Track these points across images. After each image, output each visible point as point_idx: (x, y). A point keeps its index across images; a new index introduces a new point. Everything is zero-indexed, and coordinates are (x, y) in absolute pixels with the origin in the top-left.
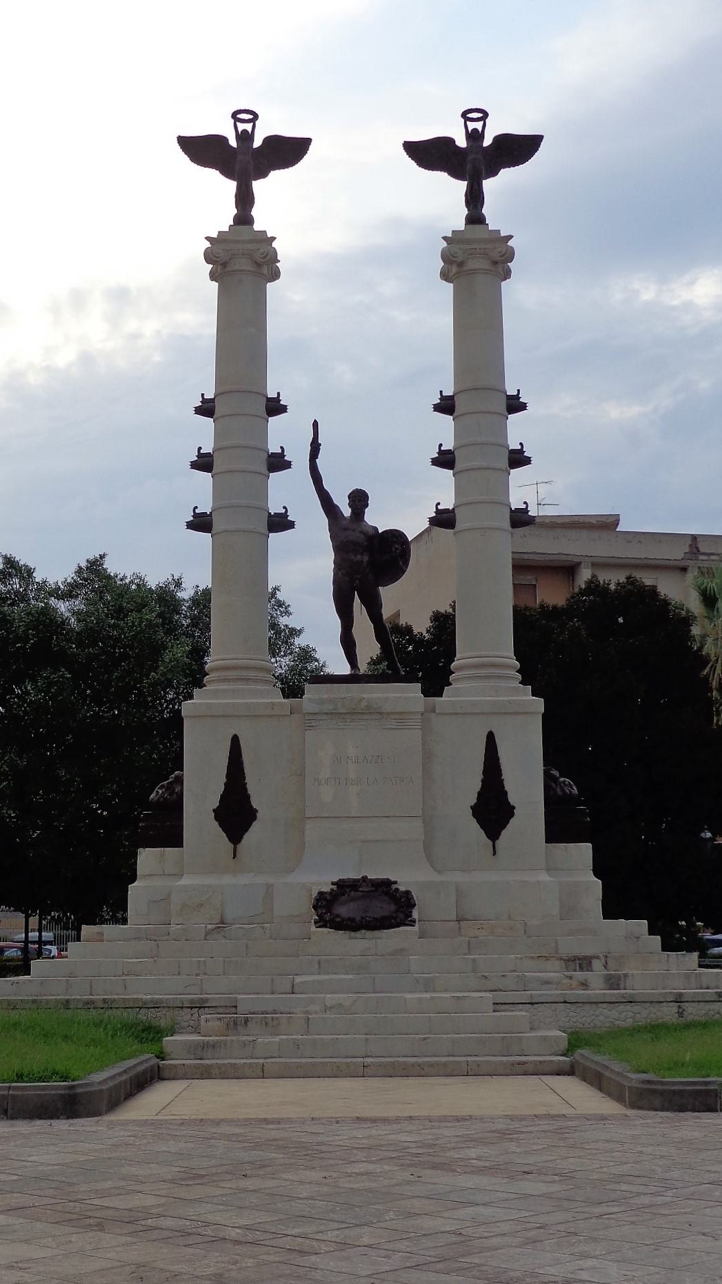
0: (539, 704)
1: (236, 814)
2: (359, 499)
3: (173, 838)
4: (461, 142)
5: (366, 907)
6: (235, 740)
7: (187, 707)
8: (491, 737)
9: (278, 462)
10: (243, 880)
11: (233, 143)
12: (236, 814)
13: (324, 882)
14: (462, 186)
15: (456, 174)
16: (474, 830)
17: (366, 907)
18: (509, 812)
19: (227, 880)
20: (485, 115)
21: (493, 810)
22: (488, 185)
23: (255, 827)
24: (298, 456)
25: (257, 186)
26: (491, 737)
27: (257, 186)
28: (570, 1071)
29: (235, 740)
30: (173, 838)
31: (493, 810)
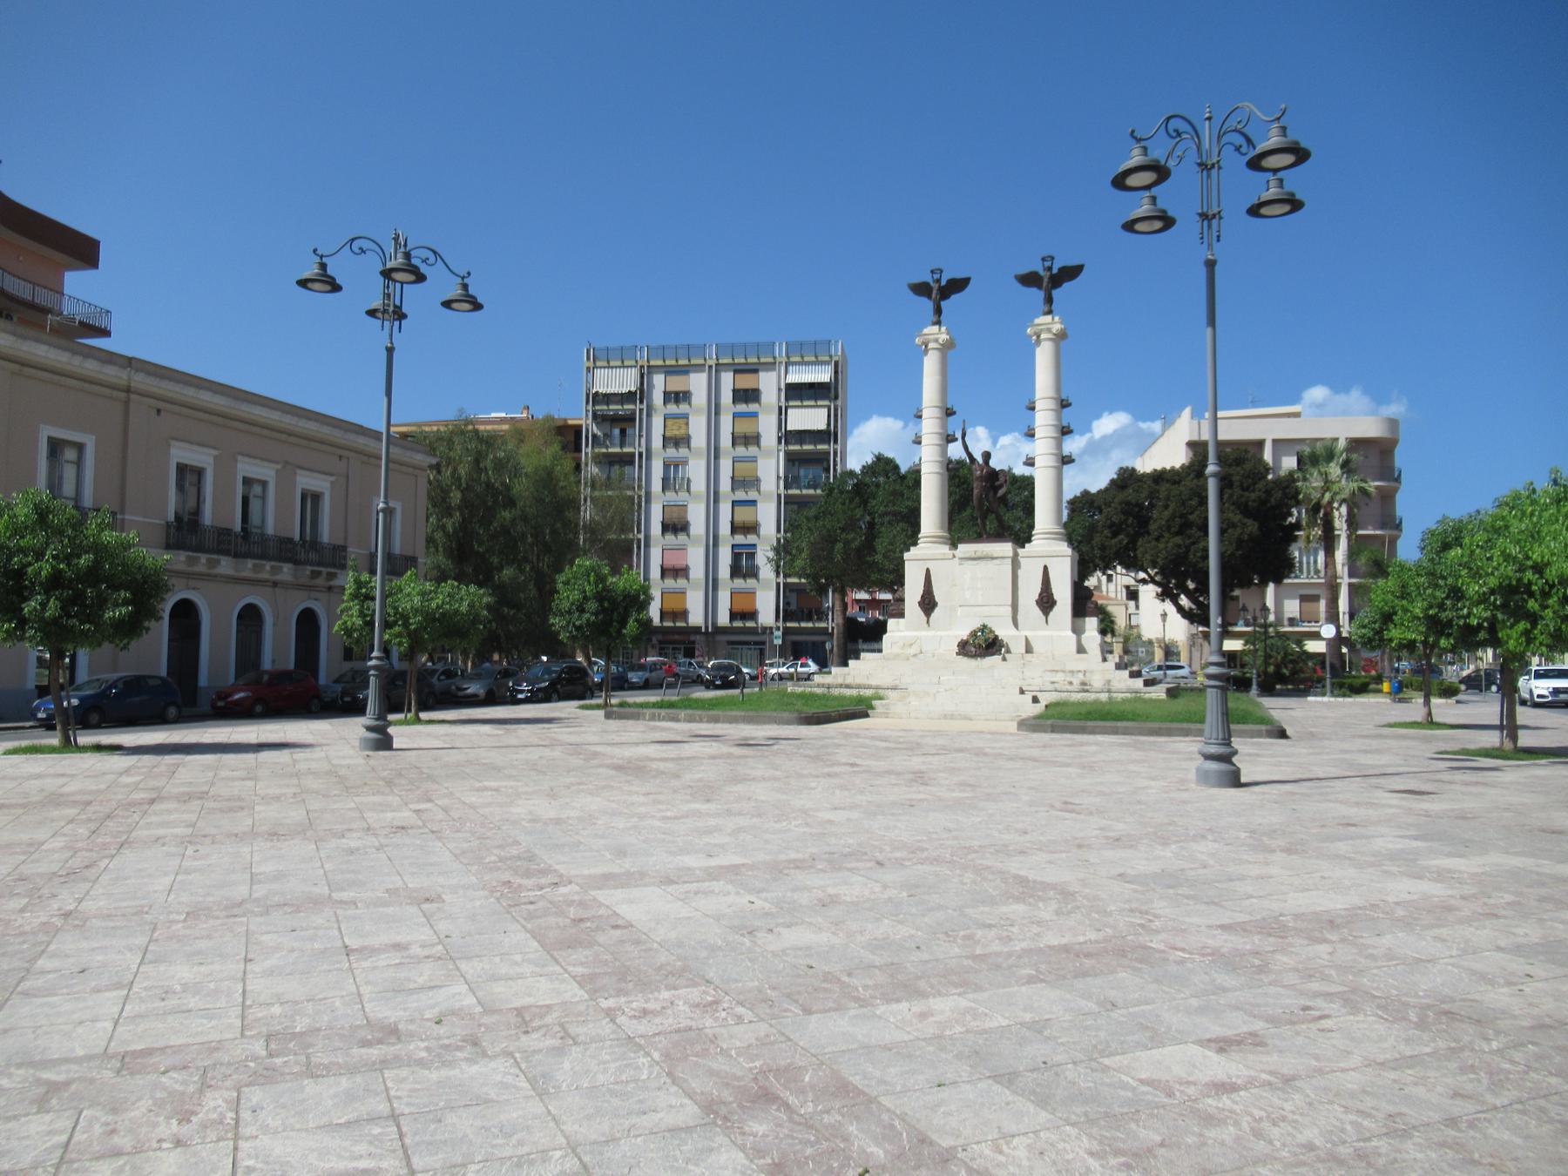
0: (1069, 551)
2: (987, 456)
3: (901, 615)
4: (1042, 273)
5: (984, 645)
6: (928, 571)
7: (906, 555)
8: (1046, 568)
9: (950, 439)
10: (930, 633)
12: (928, 604)
13: (964, 634)
15: (1039, 287)
16: (1037, 611)
17: (984, 645)
19: (924, 633)
22: (1055, 293)
23: (937, 610)
24: (959, 435)
25: (943, 304)
26: (1046, 568)
27: (943, 304)
29: (928, 571)
30: (901, 615)
31: (1046, 602)
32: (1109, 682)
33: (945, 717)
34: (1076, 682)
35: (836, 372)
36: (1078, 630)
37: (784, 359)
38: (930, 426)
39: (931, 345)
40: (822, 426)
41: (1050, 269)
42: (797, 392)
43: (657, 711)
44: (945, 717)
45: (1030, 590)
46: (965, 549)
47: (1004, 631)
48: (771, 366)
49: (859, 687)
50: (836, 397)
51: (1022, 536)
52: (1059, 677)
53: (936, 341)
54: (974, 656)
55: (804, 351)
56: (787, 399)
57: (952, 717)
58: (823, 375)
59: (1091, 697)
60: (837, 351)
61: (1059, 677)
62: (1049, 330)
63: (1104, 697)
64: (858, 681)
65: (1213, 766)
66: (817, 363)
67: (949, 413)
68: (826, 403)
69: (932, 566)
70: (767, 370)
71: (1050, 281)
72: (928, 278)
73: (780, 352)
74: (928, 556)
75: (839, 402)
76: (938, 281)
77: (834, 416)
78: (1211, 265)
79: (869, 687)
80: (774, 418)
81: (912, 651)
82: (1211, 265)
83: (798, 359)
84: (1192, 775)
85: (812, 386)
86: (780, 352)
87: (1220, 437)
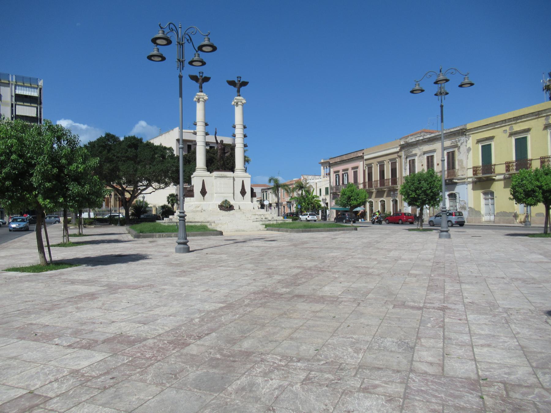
1: (204, 192)
3: (192, 196)
4: (237, 82)
5: (226, 207)
9: (207, 134)
10: (205, 203)
11: (199, 77)
12: (204, 192)
13: (219, 203)
14: (236, 89)
18: (246, 193)
20: (240, 78)
21: (243, 192)
23: (207, 195)
28: (267, 230)
30: (192, 196)
31: (243, 192)
32: (273, 218)
33: (237, 231)
34: (264, 218)
35: (40, 93)
36: (252, 201)
37: (14, 83)
38: (200, 128)
39: (201, 100)
40: (35, 115)
41: (240, 81)
42: (21, 99)
43: (161, 234)
44: (237, 231)
45: (238, 189)
46: (215, 173)
47: (232, 202)
48: (8, 85)
49: (195, 222)
50: (41, 104)
51: (232, 169)
52: (257, 217)
53: (203, 98)
54: (224, 210)
55: (23, 81)
56: (16, 101)
57: (239, 231)
58: (34, 93)
59: (271, 222)
60: (41, 83)
61: (257, 217)
62: (241, 102)
63: (275, 222)
64: (193, 220)
65: (182, 246)
66: (31, 87)
67: (206, 125)
68: (36, 105)
69: (204, 178)
70: (5, 86)
71: (238, 85)
72: (198, 75)
73: (12, 79)
74: (200, 175)
75: (42, 106)
76: (202, 76)
77: (39, 112)
78: (442, 106)
79: (199, 222)
80: (9, 108)
81: (199, 209)
82: (442, 106)
83: (21, 84)
84: (174, 250)
85: (26, 96)
86: (12, 79)
87: (184, 138)
